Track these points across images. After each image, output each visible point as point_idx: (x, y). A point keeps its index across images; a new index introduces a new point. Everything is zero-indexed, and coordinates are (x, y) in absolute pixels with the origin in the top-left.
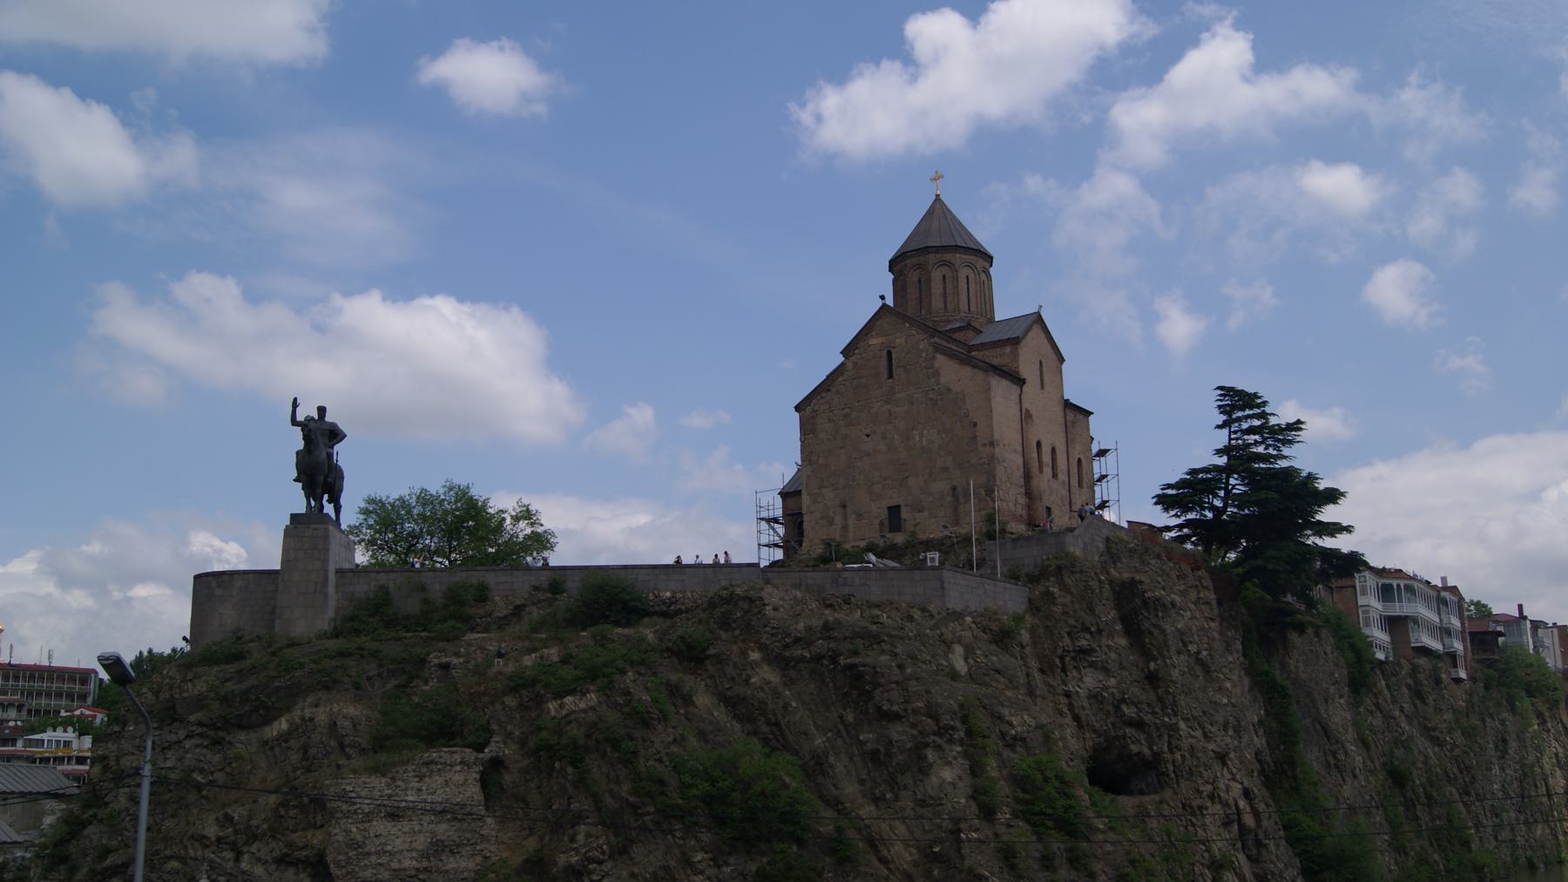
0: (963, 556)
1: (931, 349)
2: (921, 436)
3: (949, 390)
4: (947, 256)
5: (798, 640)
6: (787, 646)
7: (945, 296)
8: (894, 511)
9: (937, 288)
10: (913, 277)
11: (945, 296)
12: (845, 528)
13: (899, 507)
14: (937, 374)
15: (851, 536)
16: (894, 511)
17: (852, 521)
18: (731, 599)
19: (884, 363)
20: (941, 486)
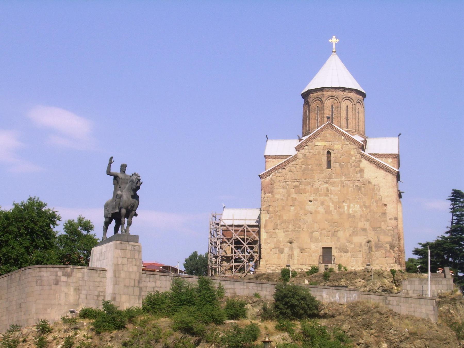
0: (379, 284)
1: (359, 156)
2: (349, 207)
3: (369, 182)
4: (351, 95)
5: (408, 338)
6: (401, 342)
7: (347, 120)
8: (327, 251)
9: (344, 114)
10: (328, 103)
11: (347, 120)
12: (291, 256)
13: (331, 248)
14: (362, 171)
15: (296, 262)
16: (327, 251)
17: (296, 252)
18: (367, 311)
19: (325, 158)
20: (360, 239)
